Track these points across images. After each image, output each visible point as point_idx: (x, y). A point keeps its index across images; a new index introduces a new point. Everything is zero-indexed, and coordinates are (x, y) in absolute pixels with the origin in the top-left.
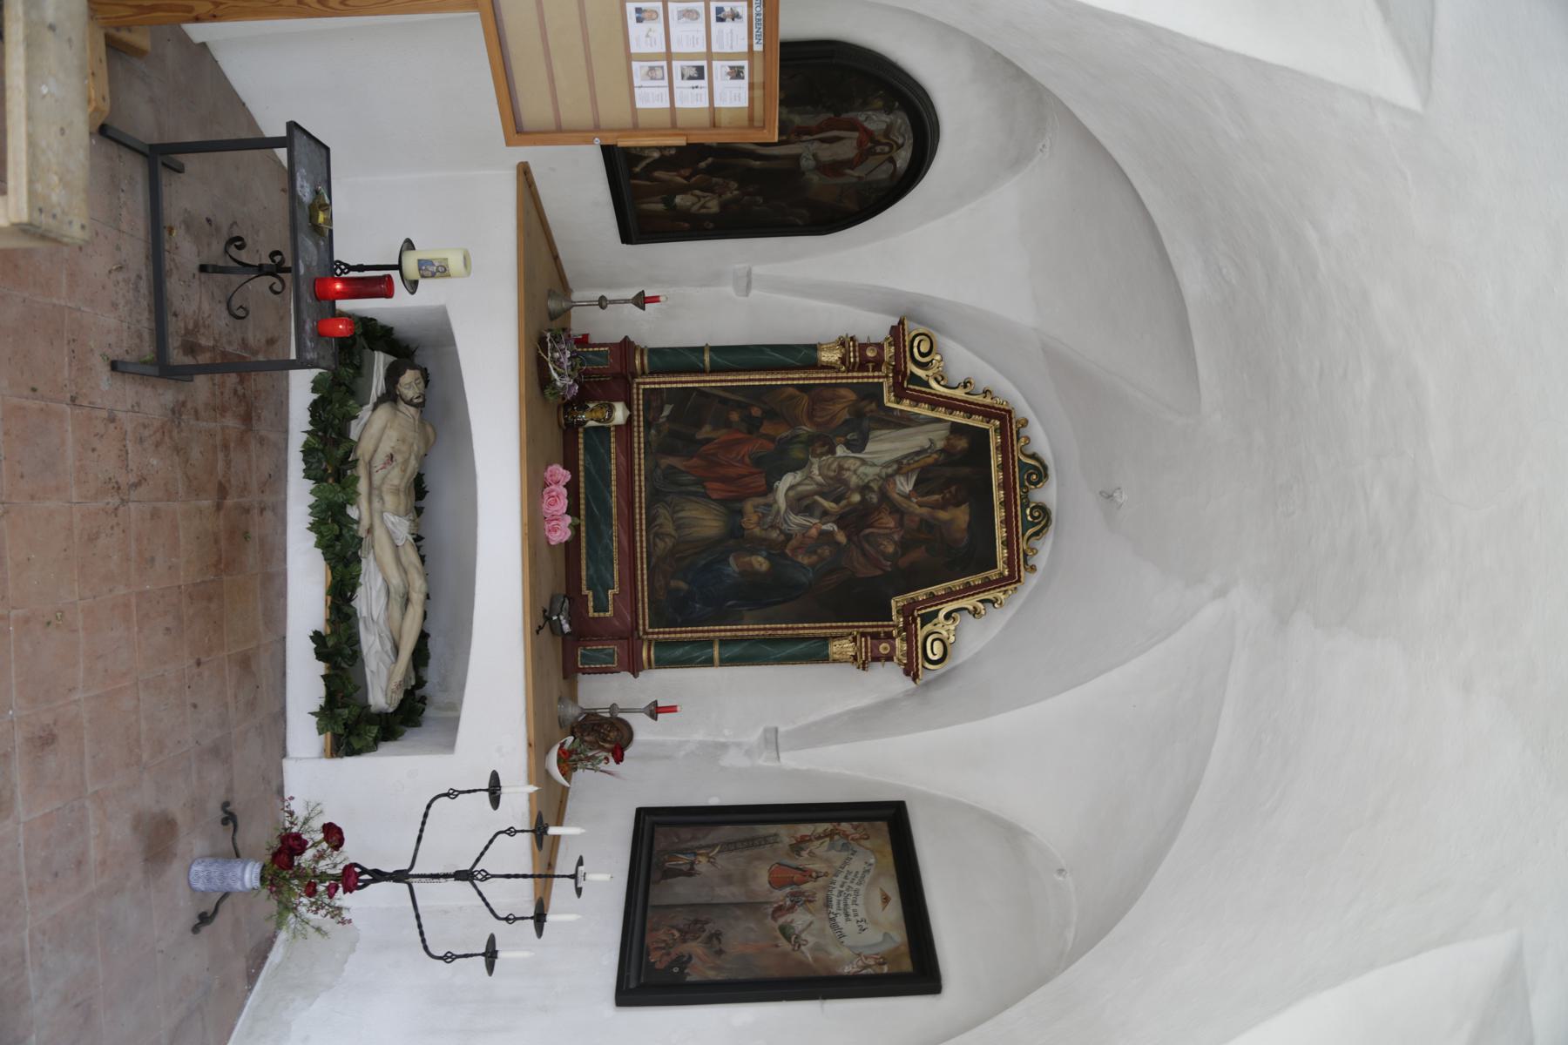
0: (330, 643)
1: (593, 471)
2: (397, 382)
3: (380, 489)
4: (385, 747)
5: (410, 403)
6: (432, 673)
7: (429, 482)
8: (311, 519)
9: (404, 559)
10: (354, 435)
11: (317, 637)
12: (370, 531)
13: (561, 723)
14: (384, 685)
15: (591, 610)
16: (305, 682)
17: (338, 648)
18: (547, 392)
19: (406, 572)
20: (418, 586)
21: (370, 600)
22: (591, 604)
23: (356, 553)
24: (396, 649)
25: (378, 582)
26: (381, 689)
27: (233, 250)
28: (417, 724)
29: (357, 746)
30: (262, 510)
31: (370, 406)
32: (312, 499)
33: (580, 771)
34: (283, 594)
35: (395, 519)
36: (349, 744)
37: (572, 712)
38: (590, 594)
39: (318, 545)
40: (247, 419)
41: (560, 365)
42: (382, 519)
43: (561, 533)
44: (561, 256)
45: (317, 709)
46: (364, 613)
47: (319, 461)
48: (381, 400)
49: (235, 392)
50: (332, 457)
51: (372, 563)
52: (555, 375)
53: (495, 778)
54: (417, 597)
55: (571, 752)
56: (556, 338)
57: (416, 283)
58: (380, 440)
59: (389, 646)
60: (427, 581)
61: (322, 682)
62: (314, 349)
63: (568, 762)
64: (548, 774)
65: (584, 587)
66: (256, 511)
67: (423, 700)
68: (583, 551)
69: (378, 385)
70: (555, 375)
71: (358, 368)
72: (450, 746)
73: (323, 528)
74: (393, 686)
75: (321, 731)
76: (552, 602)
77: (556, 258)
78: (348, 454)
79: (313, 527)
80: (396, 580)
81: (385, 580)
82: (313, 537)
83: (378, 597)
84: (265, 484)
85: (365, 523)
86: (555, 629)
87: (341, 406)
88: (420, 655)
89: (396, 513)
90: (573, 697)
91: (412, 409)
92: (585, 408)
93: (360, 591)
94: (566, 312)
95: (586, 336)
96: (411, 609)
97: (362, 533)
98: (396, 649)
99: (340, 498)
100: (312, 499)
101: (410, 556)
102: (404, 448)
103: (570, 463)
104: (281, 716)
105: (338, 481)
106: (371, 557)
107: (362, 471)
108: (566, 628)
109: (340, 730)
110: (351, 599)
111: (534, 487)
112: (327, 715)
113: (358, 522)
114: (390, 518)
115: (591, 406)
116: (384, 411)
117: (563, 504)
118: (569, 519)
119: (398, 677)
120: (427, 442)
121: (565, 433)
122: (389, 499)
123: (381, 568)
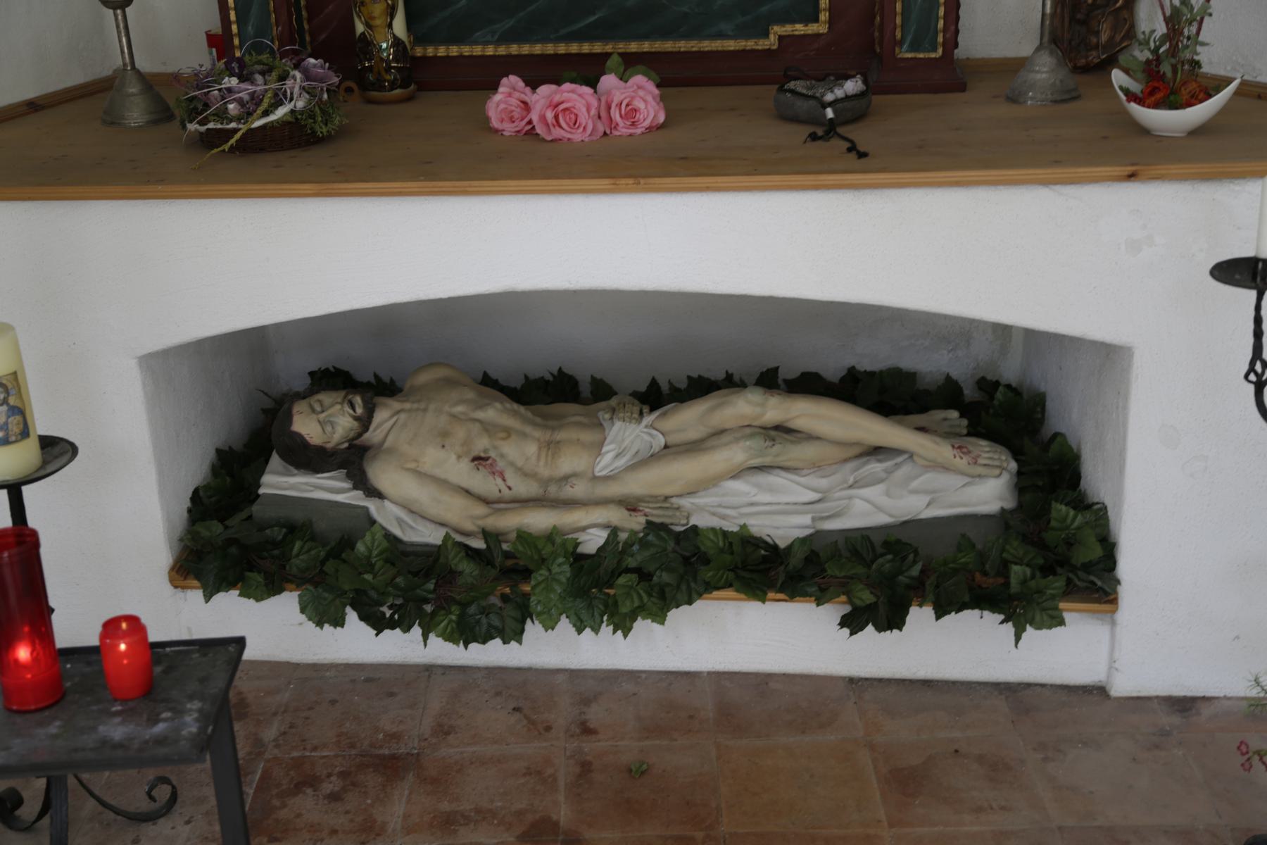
0: (866, 597)
1: (509, 23)
2: (321, 450)
3: (545, 483)
4: (1095, 481)
5: (365, 422)
6: (932, 364)
7: (542, 365)
8: (606, 630)
9: (693, 434)
10: (431, 536)
11: (853, 623)
12: (631, 505)
13: (1068, 96)
14: (959, 480)
15: (813, 28)
16: (951, 646)
17: (877, 576)
18: (322, 130)
19: (723, 432)
20: (750, 406)
21: (778, 506)
22: (800, 29)
23: (678, 537)
24: (876, 451)
25: (741, 488)
26: (966, 486)
27: (28, 811)
28: (1039, 401)
29: (1097, 552)
30: (587, 730)
31: (372, 505)
32: (565, 625)
33: (1203, 55)
34: (760, 682)
35: (610, 450)
36: (1088, 567)
37: (1045, 71)
38: (778, 30)
39: (660, 617)
40: (392, 766)
41: (256, 99)
42: (611, 474)
43: (640, 97)
44: (30, 93)
45: (1009, 628)
46: (806, 520)
47: (485, 611)
48: (361, 482)
49: (334, 797)
50: (477, 583)
51: (700, 500)
52: (281, 112)
53: (1234, 271)
54: (776, 408)
55: (1151, 72)
56: (196, 109)
57: (48, 443)
58: (443, 483)
59: (875, 467)
60: (742, 385)
61: (951, 619)
62: (179, 712)
63: (1173, 80)
64: (1198, 132)
65: (762, 44)
66: (590, 747)
67: (988, 386)
68: (683, 46)
69: (327, 488)
70: (281, 112)
71: (293, 529)
72: (1108, 359)
73: (625, 609)
74: (962, 462)
75: (1057, 621)
76: (795, 119)
77: (33, 107)
78: (471, 553)
79: (623, 625)
80: (736, 454)
81: (737, 474)
82: (642, 626)
83: (771, 489)
84: (533, 723)
85: (616, 516)
86: (854, 111)
87: (370, 567)
88: (887, 393)
89: (597, 448)
90: (1013, 66)
91: (381, 416)
92: (366, 44)
93: (762, 526)
94: (149, 83)
95: (212, 40)
96: (798, 424)
97: (636, 523)
98: (876, 451)
99: (562, 569)
100: (565, 625)
101: (688, 419)
102: (460, 433)
103: (485, 77)
104: (1015, 694)
105: (526, 573)
106: (685, 502)
107: (510, 521)
108: (852, 86)
109: (1058, 583)
110: (775, 547)
111: (538, 162)
112: (1023, 608)
113: (614, 531)
114: (607, 462)
115: (360, 28)
116: (383, 475)
117: (574, 95)
118: (609, 81)
119: (943, 450)
120: (450, 383)
121: (422, 87)
122: (569, 462)
123: (711, 482)
